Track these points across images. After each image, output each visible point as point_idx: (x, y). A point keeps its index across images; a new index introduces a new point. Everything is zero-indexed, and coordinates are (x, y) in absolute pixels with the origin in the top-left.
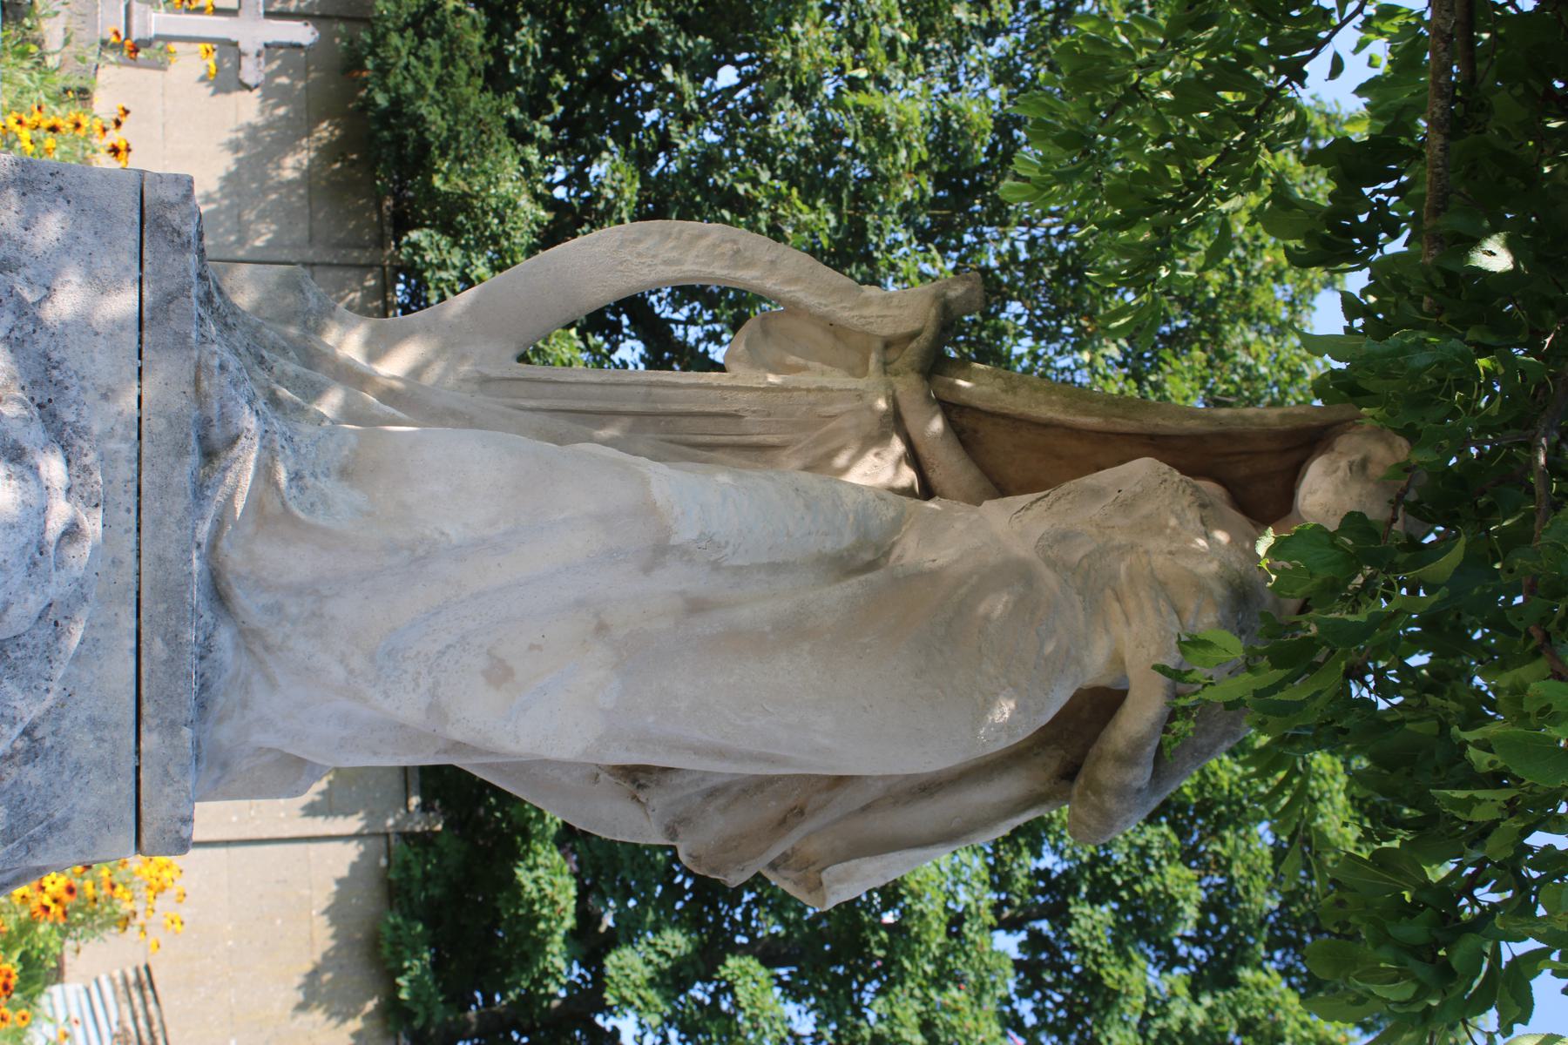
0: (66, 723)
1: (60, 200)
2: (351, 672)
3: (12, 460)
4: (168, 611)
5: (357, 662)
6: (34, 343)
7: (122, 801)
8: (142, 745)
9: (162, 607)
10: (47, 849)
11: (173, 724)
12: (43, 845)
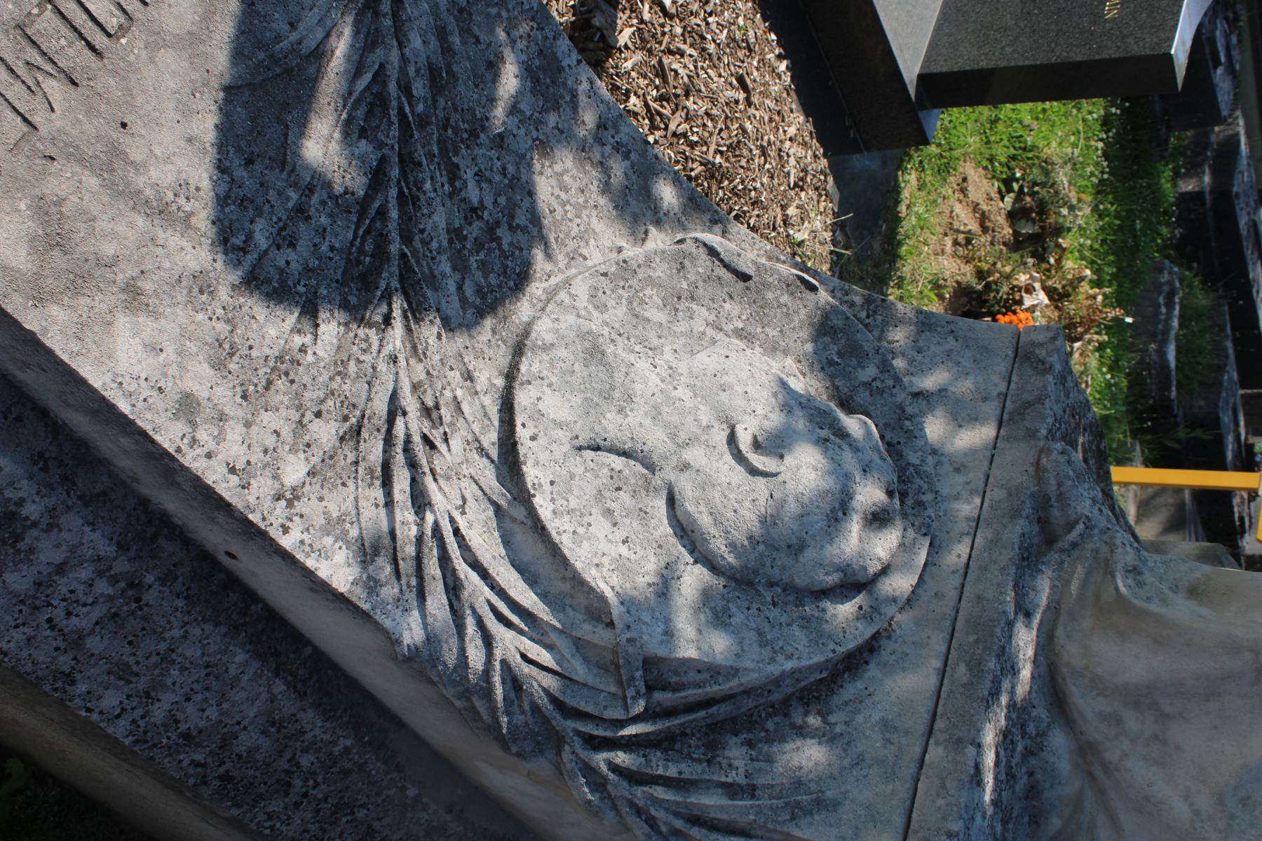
0: (860, 718)
1: (950, 339)
2: (1197, 813)
4: (976, 642)
5: (1204, 802)
6: (892, 395)
7: (895, 802)
8: (927, 757)
9: (972, 638)
10: (811, 824)
11: (960, 740)
12: (808, 818)
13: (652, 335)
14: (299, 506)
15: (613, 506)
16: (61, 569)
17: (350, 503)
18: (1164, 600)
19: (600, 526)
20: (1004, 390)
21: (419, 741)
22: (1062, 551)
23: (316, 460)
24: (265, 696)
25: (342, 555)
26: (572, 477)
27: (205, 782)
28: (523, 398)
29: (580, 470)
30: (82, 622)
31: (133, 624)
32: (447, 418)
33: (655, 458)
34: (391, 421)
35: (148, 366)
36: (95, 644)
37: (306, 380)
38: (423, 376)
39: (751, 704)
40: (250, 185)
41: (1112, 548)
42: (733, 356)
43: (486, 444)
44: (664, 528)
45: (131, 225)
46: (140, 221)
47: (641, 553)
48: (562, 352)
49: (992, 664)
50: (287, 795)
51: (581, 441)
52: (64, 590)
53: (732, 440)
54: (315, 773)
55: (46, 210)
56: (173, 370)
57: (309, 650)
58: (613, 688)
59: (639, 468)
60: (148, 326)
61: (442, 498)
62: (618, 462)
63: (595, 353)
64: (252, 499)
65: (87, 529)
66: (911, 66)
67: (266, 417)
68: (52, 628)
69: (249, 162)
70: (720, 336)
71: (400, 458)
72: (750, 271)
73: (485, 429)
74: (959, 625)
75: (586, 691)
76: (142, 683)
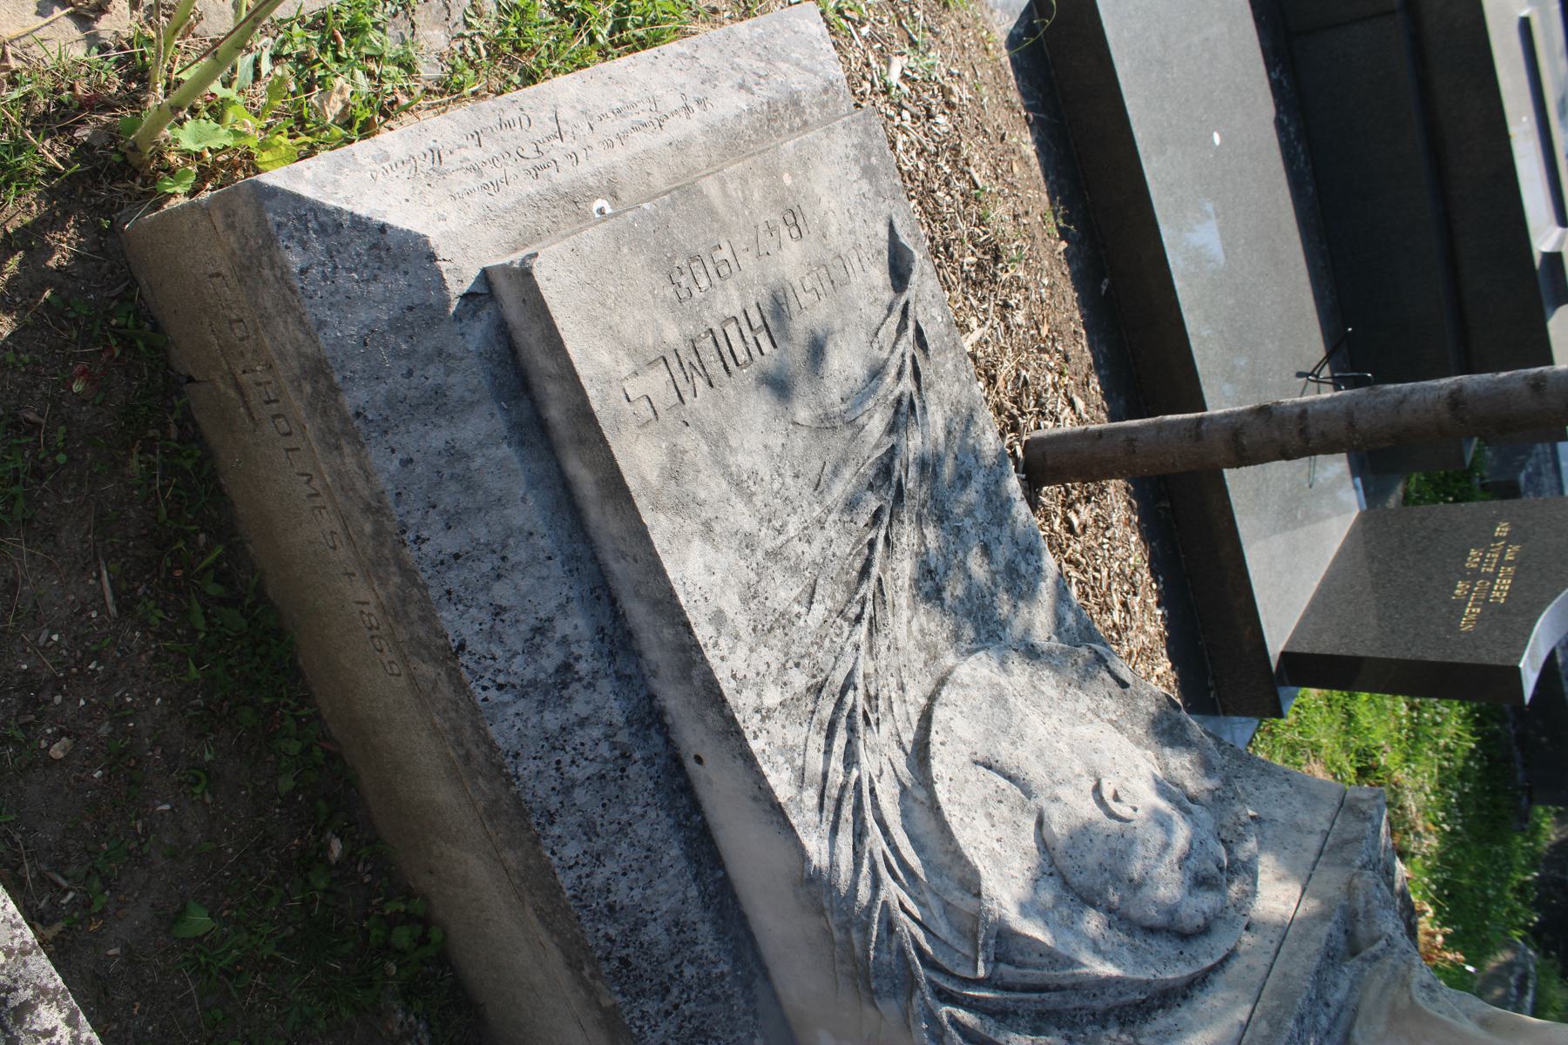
4: (1279, 1007)
9: (1275, 1003)
13: (1044, 703)
14: (769, 724)
15: (994, 812)
16: (583, 722)
17: (801, 741)
18: (1454, 1016)
19: (982, 823)
20: (1326, 826)
21: (776, 999)
22: (1364, 959)
23: (788, 696)
24: (680, 895)
25: (787, 775)
26: (967, 781)
27: (607, 959)
28: (939, 714)
29: (973, 779)
30: (578, 773)
31: (612, 790)
32: (882, 708)
33: (1033, 786)
34: (844, 692)
35: (703, 580)
36: (580, 796)
37: (795, 637)
38: (872, 671)
39: (1078, 1003)
40: (792, 493)
41: (1410, 967)
44: (1030, 841)
45: (719, 485)
46: (724, 485)
47: (1009, 853)
48: (974, 693)
49: (1291, 1024)
50: (663, 1000)
51: (978, 757)
52: (578, 741)
53: (1097, 789)
54: (691, 988)
55: (675, 453)
56: (717, 590)
57: (720, 874)
58: (967, 951)
59: (1018, 791)
61: (868, 764)
62: (1004, 783)
63: (1000, 699)
64: (741, 704)
65: (612, 696)
66: (1276, 641)
67: (764, 650)
68: (558, 769)
69: (797, 476)
71: (844, 720)
72: (1129, 680)
74: (1265, 992)
75: (944, 948)
76: (599, 844)
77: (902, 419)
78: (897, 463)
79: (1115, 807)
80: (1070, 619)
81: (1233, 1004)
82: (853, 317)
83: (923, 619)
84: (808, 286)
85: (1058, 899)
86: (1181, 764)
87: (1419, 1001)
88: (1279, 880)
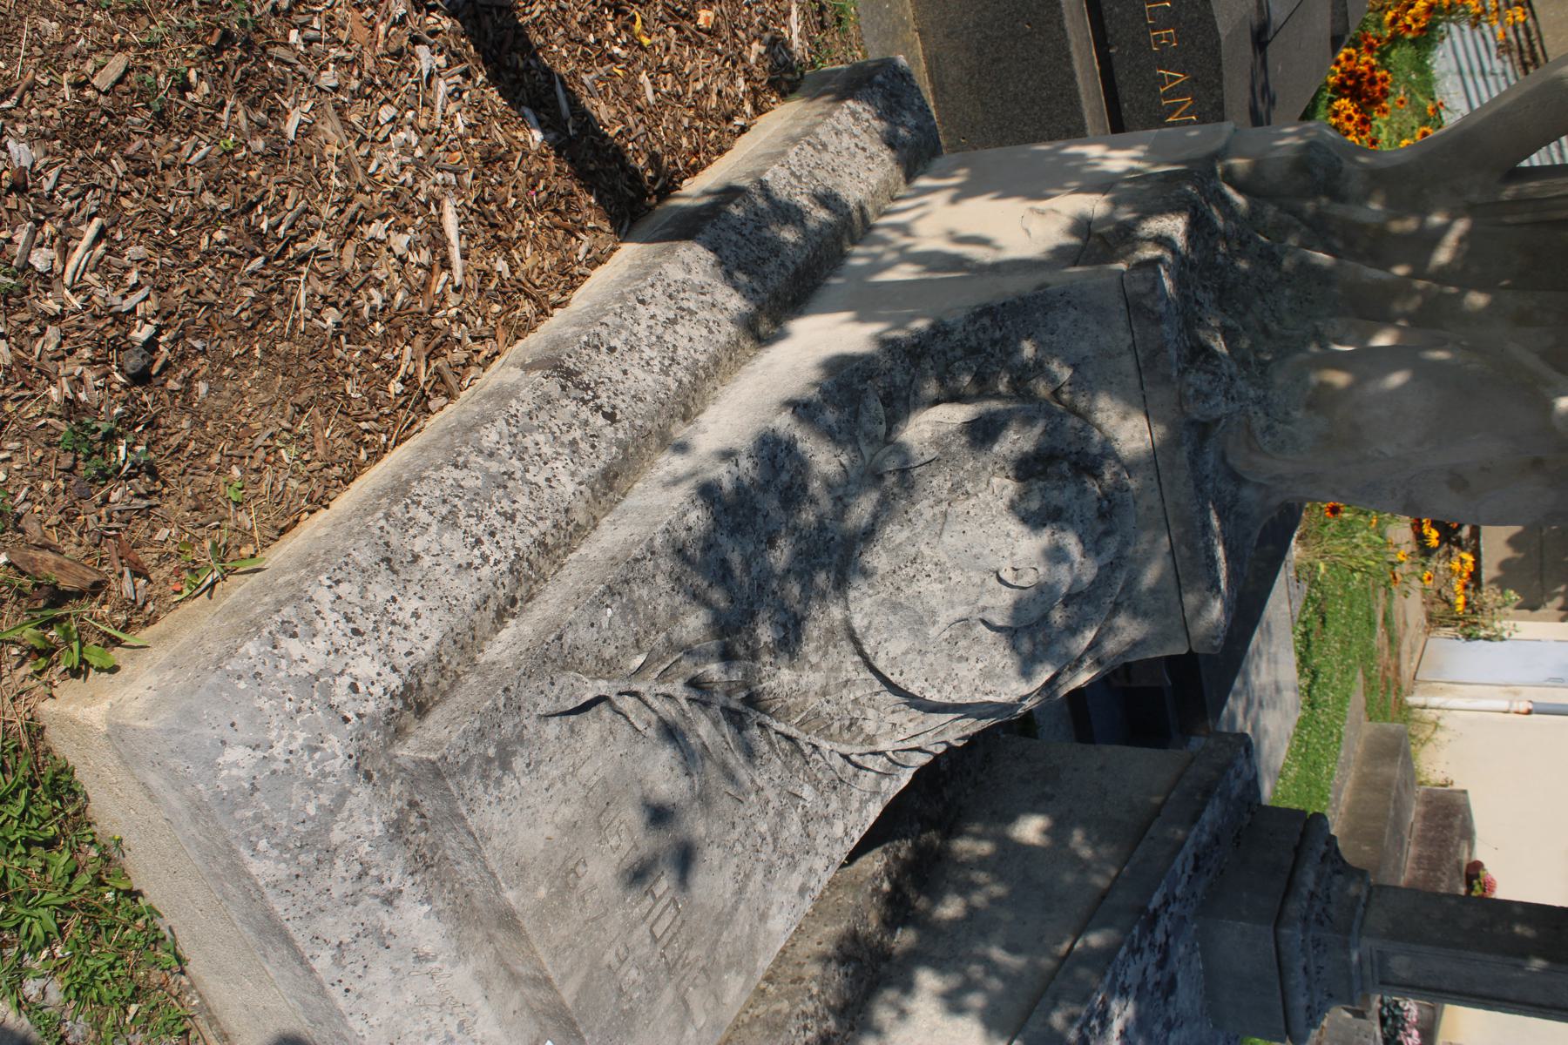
1: (1070, 310)
3: (1055, 521)
19: (962, 669)
20: (1129, 341)
28: (880, 664)
42: (967, 529)
43: (877, 689)
46: (742, 907)
53: (1000, 580)
60: (774, 909)
70: (945, 504)
73: (871, 686)
77: (704, 698)
78: (734, 705)
79: (1020, 583)
80: (830, 416)
81: (1154, 541)
82: (628, 767)
83: (813, 645)
84: (613, 842)
85: (1032, 637)
86: (1016, 441)
87: (1266, 448)
88: (1124, 418)
